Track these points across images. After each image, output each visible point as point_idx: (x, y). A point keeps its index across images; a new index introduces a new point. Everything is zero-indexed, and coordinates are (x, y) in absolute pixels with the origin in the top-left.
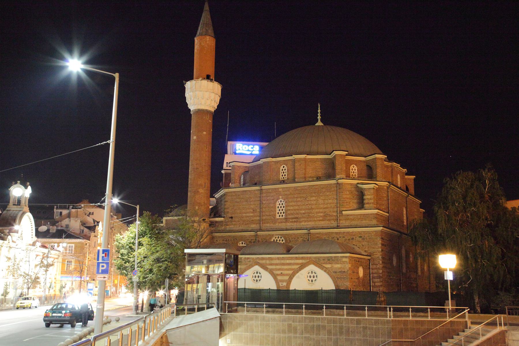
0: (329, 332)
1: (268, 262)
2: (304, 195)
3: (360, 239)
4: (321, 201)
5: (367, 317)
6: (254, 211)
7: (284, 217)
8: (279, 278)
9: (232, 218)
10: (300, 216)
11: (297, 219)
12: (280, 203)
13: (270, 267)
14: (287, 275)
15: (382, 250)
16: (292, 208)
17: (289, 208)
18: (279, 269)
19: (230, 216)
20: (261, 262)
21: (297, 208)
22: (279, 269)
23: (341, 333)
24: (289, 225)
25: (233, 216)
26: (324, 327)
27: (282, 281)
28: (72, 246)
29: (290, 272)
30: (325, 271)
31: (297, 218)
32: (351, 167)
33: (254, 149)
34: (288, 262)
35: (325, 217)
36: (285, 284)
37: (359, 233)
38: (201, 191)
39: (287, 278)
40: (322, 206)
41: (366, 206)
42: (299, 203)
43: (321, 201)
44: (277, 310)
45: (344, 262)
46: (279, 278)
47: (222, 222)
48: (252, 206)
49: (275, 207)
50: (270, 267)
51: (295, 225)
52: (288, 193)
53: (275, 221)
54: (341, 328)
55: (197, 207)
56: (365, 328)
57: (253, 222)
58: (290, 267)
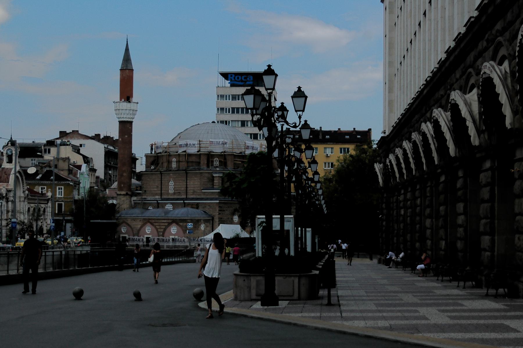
1: (154, 221)
3: (208, 207)
4: (192, 183)
6: (157, 187)
8: (159, 230)
9: (145, 191)
10: (181, 192)
12: (171, 183)
13: (155, 224)
15: (219, 214)
18: (159, 225)
19: (144, 189)
24: (176, 197)
25: (146, 189)
27: (160, 232)
28: (62, 188)
31: (179, 193)
33: (248, 79)
34: (163, 221)
35: (194, 192)
36: (161, 233)
37: (209, 203)
38: (125, 174)
39: (162, 230)
41: (215, 187)
43: (192, 183)
47: (140, 193)
48: (156, 184)
49: (168, 185)
50: (155, 224)
51: (179, 197)
53: (168, 194)
57: (156, 194)
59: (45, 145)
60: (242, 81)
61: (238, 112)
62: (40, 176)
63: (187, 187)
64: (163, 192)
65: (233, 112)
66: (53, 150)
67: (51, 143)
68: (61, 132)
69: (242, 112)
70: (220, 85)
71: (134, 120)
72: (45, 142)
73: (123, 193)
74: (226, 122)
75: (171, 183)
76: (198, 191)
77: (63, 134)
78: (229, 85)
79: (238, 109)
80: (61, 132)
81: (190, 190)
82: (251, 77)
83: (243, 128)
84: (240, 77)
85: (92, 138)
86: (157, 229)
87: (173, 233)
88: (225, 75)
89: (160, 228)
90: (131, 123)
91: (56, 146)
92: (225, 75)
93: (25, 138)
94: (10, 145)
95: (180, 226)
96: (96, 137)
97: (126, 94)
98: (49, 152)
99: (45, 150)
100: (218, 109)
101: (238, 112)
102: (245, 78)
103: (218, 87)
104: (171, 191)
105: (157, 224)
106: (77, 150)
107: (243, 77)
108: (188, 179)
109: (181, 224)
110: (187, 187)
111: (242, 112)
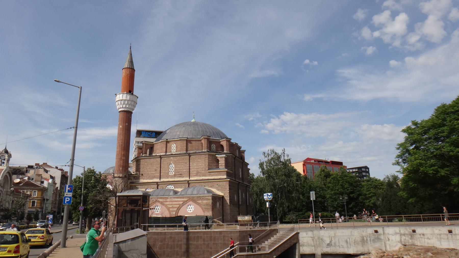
0: (204, 240)
1: (164, 200)
2: (186, 161)
5: (441, 214)
7: (173, 174)
8: (171, 209)
11: (181, 175)
13: (165, 203)
14: (176, 207)
16: (178, 169)
17: (176, 168)
18: (171, 205)
20: (160, 200)
21: (181, 168)
22: (171, 205)
23: (211, 240)
25: (143, 173)
26: (201, 237)
27: (173, 211)
29: (178, 206)
30: (198, 205)
31: (181, 174)
32: (212, 145)
36: (174, 213)
39: (176, 209)
40: (196, 167)
42: (183, 166)
44: (170, 228)
45: (209, 199)
46: (171, 209)
48: (155, 168)
52: (176, 160)
54: (211, 237)
55: (121, 168)
56: (224, 236)
58: (177, 203)
62: (22, 184)
63: (189, 169)
64: (162, 174)
67: (31, 167)
71: (133, 112)
72: (27, 166)
73: (121, 175)
76: (203, 172)
81: (193, 171)
82: (154, 133)
86: (168, 209)
87: (189, 212)
89: (173, 207)
90: (131, 113)
94: (4, 152)
95: (198, 204)
98: (29, 172)
99: (27, 171)
104: (172, 173)
105: (168, 203)
108: (191, 161)
109: (200, 202)
110: (189, 169)
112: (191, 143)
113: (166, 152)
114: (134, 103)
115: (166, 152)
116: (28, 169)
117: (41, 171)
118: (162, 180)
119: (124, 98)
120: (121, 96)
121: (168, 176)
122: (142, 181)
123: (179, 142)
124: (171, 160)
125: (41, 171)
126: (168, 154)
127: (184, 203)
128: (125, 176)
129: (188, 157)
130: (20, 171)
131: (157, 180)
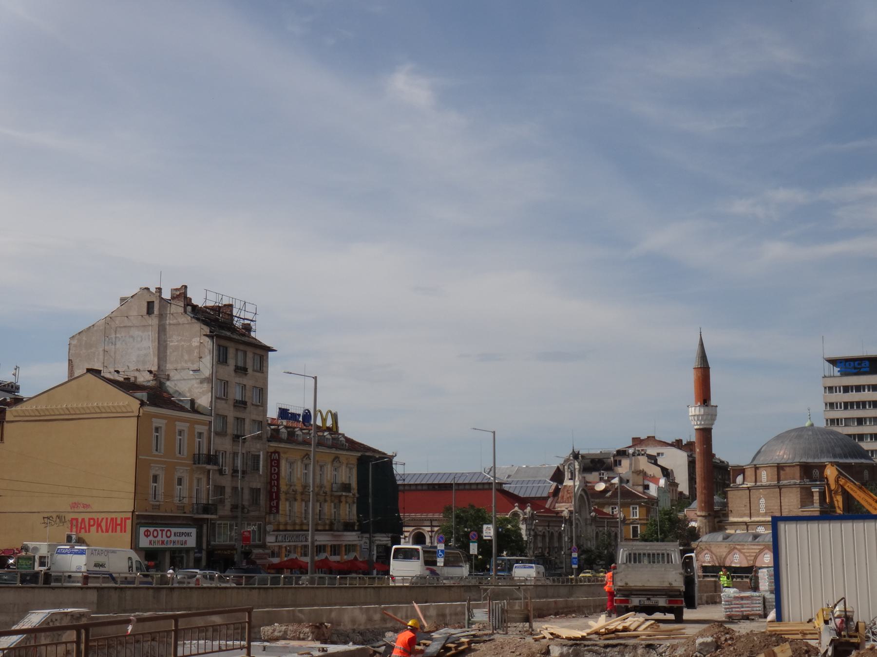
12: (762, 501)
33: (863, 365)
59: (614, 456)
60: (855, 368)
61: (852, 407)
65: (846, 408)
66: (625, 463)
67: (622, 453)
68: (633, 439)
69: (858, 407)
70: (827, 374)
74: (838, 420)
75: (762, 501)
77: (637, 441)
78: (839, 374)
79: (852, 404)
80: (633, 439)
82: (867, 363)
83: (860, 427)
84: (852, 363)
85: (672, 445)
86: (746, 557)
88: (833, 362)
91: (628, 456)
92: (833, 362)
93: (592, 448)
96: (678, 444)
97: (704, 396)
98: (620, 464)
99: (615, 461)
100: (826, 404)
101: (852, 407)
102: (859, 364)
103: (825, 377)
106: (653, 459)
107: (856, 363)
111: (858, 407)
112: (783, 470)
113: (756, 481)
114: (712, 417)
115: (756, 481)
116: (618, 458)
117: (643, 463)
118: (753, 519)
119: (697, 413)
120: (695, 410)
121: (759, 515)
122: (732, 519)
123: (769, 469)
124: (760, 494)
125: (643, 463)
126: (758, 484)
127: (761, 551)
128: (709, 515)
129: (778, 490)
130: (604, 463)
131: (747, 519)
